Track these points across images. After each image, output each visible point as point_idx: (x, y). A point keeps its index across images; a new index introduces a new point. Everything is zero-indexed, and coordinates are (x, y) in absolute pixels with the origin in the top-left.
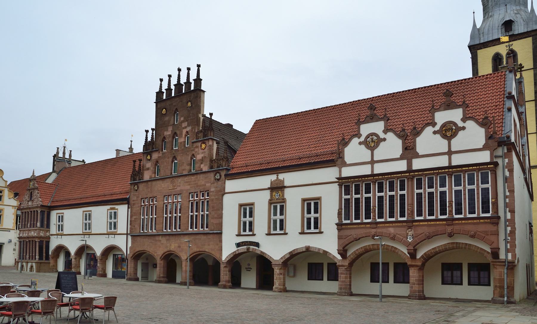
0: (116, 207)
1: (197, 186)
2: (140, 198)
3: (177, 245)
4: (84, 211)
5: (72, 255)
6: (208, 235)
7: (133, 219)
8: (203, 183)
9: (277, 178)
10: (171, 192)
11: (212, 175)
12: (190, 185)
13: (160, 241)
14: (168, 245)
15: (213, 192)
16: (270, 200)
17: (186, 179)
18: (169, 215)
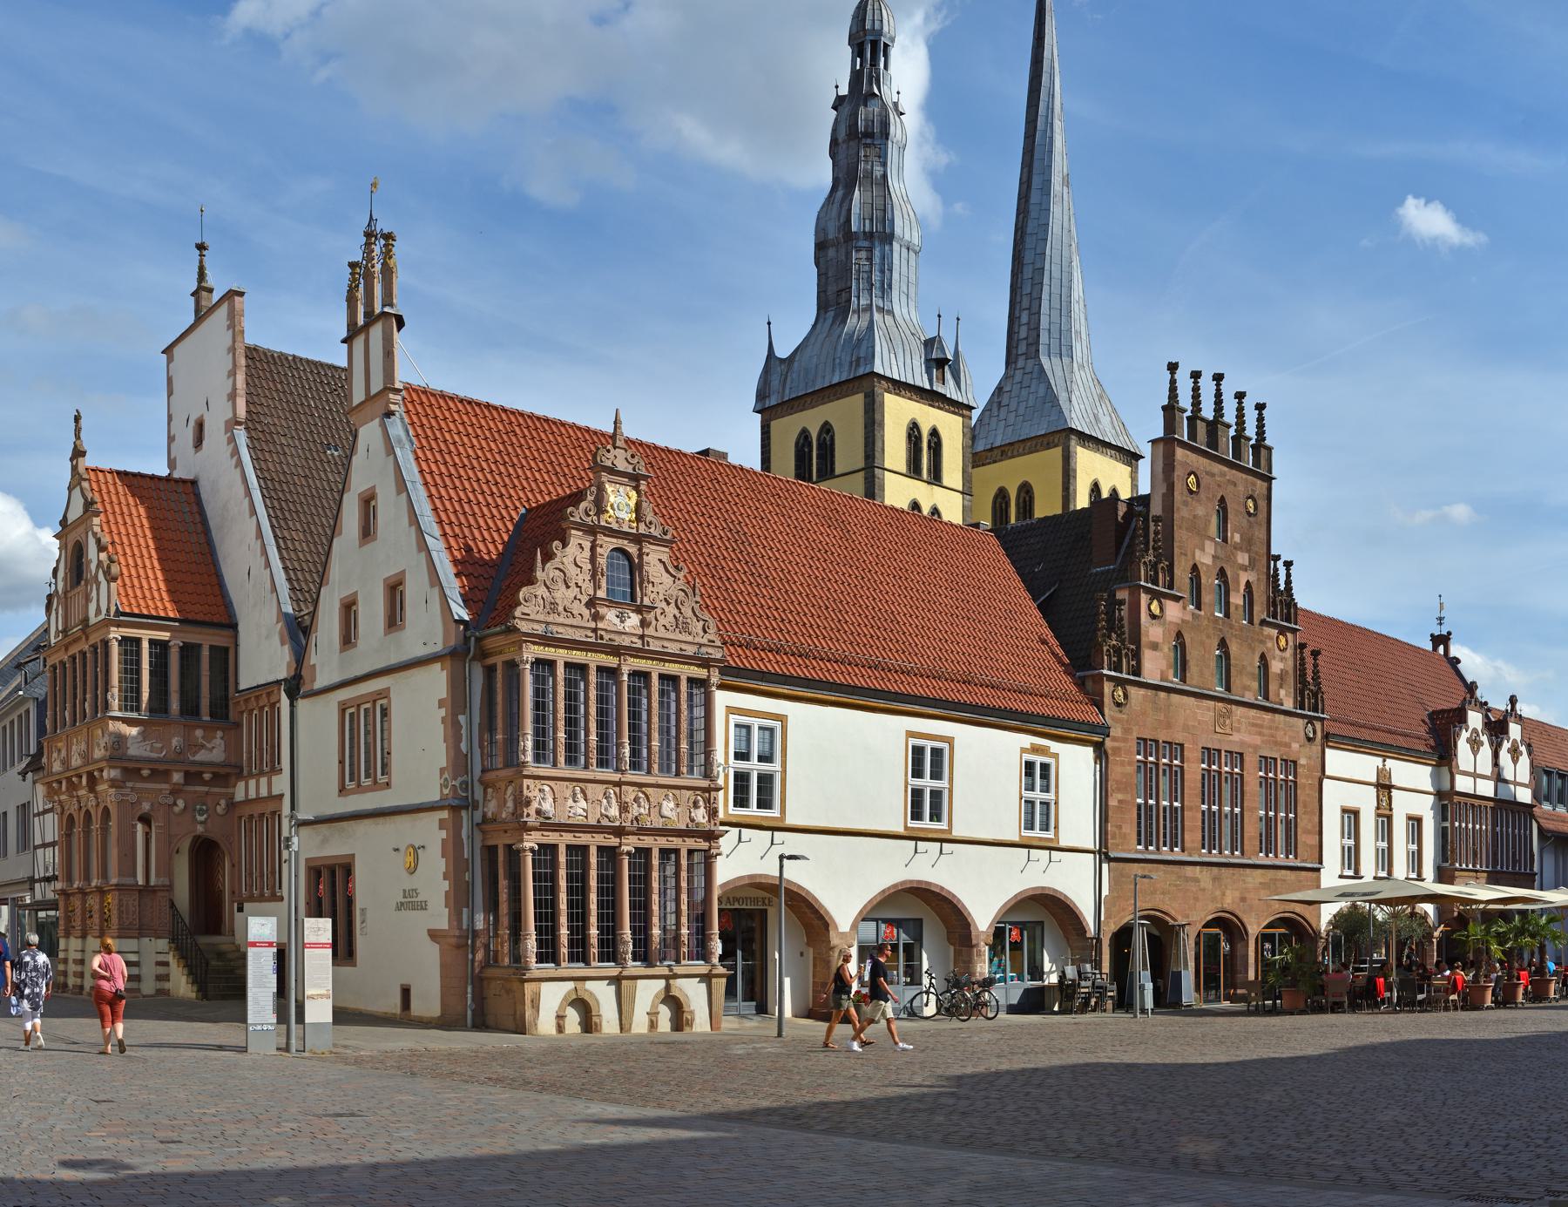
0: (1055, 746)
1: (1276, 743)
2: (1135, 735)
3: (1237, 894)
4: (910, 734)
5: (841, 929)
8: (1287, 739)
9: (1384, 765)
10: (1219, 741)
11: (1301, 722)
12: (1260, 734)
13: (1197, 880)
14: (1218, 893)
16: (1378, 808)
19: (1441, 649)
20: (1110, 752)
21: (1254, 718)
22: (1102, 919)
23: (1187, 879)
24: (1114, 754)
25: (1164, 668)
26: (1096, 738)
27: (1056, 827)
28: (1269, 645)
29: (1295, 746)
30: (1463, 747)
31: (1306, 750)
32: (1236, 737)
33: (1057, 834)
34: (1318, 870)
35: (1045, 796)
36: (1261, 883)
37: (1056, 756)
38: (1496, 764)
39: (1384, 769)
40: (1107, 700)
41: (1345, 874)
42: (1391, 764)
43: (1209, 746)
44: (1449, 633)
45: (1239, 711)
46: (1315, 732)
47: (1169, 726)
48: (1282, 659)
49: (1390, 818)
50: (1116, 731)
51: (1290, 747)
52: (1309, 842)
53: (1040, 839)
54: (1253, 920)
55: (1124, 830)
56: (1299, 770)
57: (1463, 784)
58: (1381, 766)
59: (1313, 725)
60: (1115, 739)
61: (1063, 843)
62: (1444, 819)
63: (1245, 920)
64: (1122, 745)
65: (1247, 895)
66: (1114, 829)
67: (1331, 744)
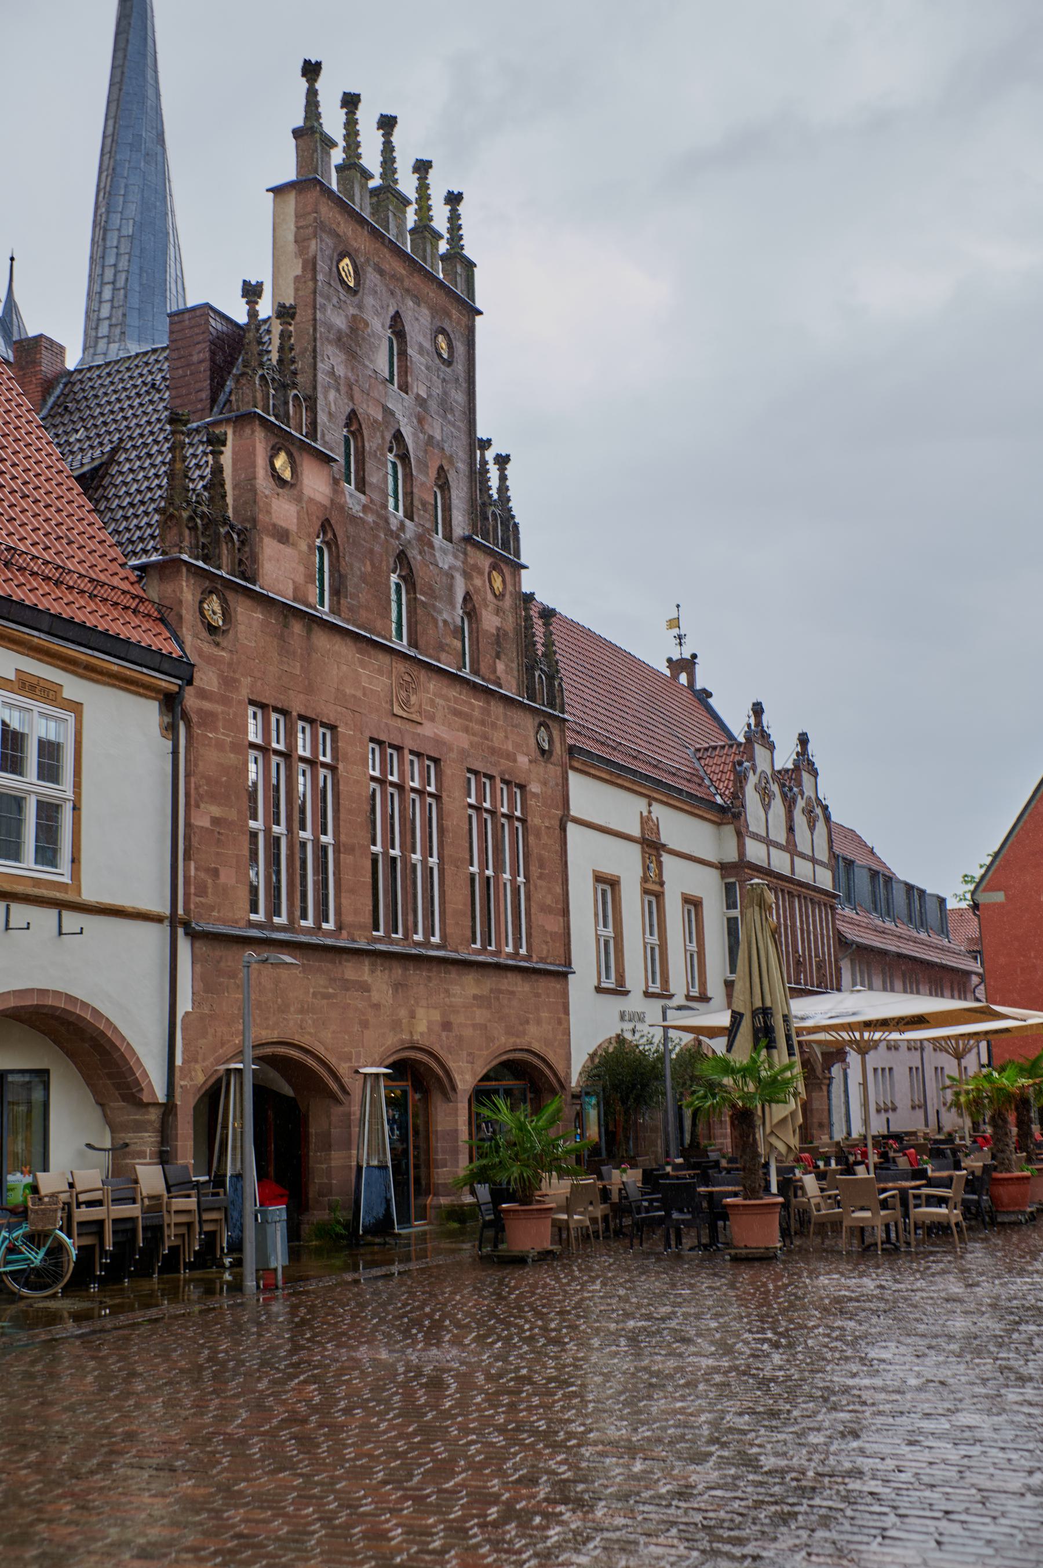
1: (493, 751)
2: (244, 693)
3: (436, 1016)
6: (345, 956)
7: (202, 821)
9: (650, 812)
11: (529, 723)
12: (466, 730)
13: (365, 988)
14: (403, 1013)
15: (535, 795)
17: (453, 692)
18: (306, 835)
19: (683, 678)
20: (195, 719)
21: (456, 700)
22: (179, 1061)
23: (347, 985)
24: (200, 725)
25: (300, 579)
26: (168, 683)
27: (75, 860)
28: (478, 582)
29: (523, 760)
30: (752, 797)
31: (540, 769)
32: (428, 730)
33: (76, 874)
34: (564, 975)
35: (48, 789)
36: (475, 997)
37: (76, 708)
38: (791, 829)
39: (649, 818)
40: (189, 615)
41: (603, 985)
42: (659, 811)
43: (383, 738)
44: (694, 656)
45: (432, 685)
46: (551, 742)
47: (310, 689)
48: (498, 611)
49: (659, 896)
50: (206, 678)
51: (515, 761)
52: (548, 928)
53: (37, 882)
54: (464, 1065)
55: (223, 879)
56: (532, 802)
57: (755, 852)
58: (645, 814)
59: (547, 727)
60: (203, 694)
61: (89, 895)
62: (731, 905)
63: (451, 1065)
64: (218, 708)
65: (452, 1018)
66: (202, 875)
67: (576, 764)
